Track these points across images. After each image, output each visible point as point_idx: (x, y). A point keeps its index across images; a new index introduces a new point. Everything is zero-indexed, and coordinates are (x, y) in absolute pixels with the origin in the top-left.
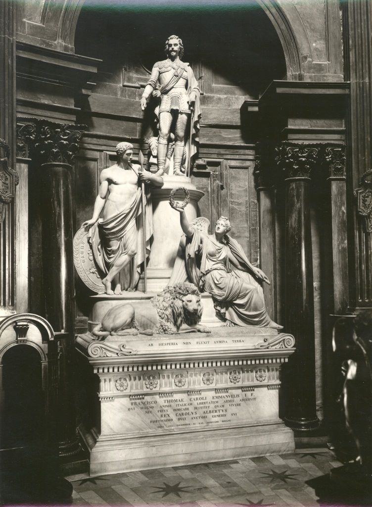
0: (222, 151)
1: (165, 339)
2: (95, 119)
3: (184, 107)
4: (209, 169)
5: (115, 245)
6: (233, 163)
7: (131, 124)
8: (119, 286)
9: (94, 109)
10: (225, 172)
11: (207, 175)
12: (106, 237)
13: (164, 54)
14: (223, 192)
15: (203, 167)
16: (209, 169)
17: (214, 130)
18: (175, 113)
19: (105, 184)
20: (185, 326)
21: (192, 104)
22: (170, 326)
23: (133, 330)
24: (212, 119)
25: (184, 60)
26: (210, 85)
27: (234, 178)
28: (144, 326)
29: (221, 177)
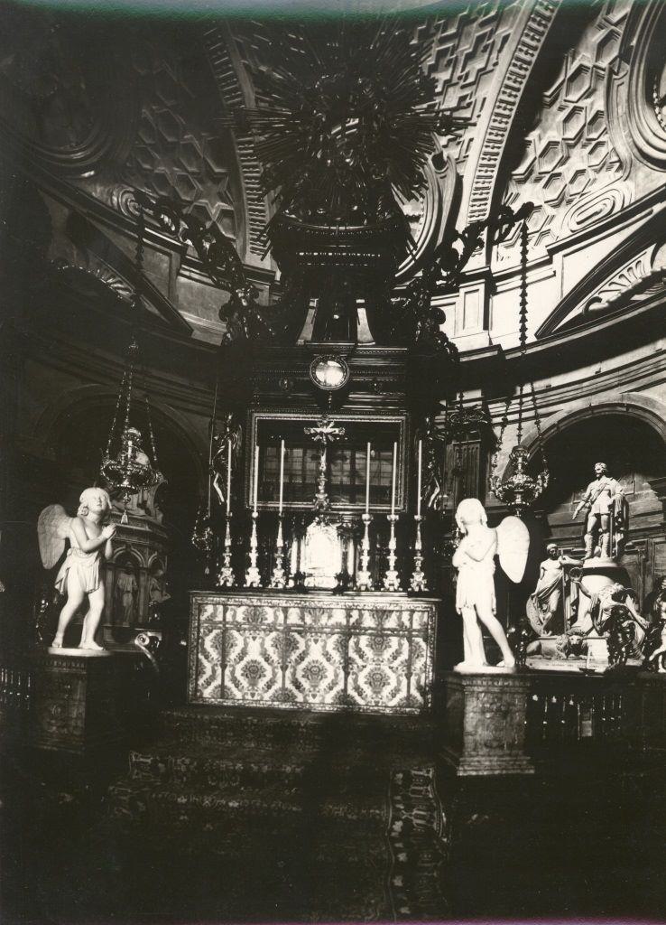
0: (647, 533)
1: (557, 662)
2: (553, 530)
3: (605, 510)
4: (637, 548)
5: (545, 607)
6: (658, 540)
7: (578, 527)
8: (550, 632)
9: (551, 524)
10: (650, 548)
11: (636, 553)
12: (543, 600)
13: (593, 477)
14: (648, 563)
15: (632, 547)
16: (637, 548)
17: (642, 518)
18: (598, 516)
19: (542, 571)
20: (572, 655)
21: (611, 507)
22: (563, 655)
23: (540, 656)
24: (641, 509)
25: (608, 476)
26: (640, 485)
27: (660, 552)
28: (547, 654)
29: (646, 553)
